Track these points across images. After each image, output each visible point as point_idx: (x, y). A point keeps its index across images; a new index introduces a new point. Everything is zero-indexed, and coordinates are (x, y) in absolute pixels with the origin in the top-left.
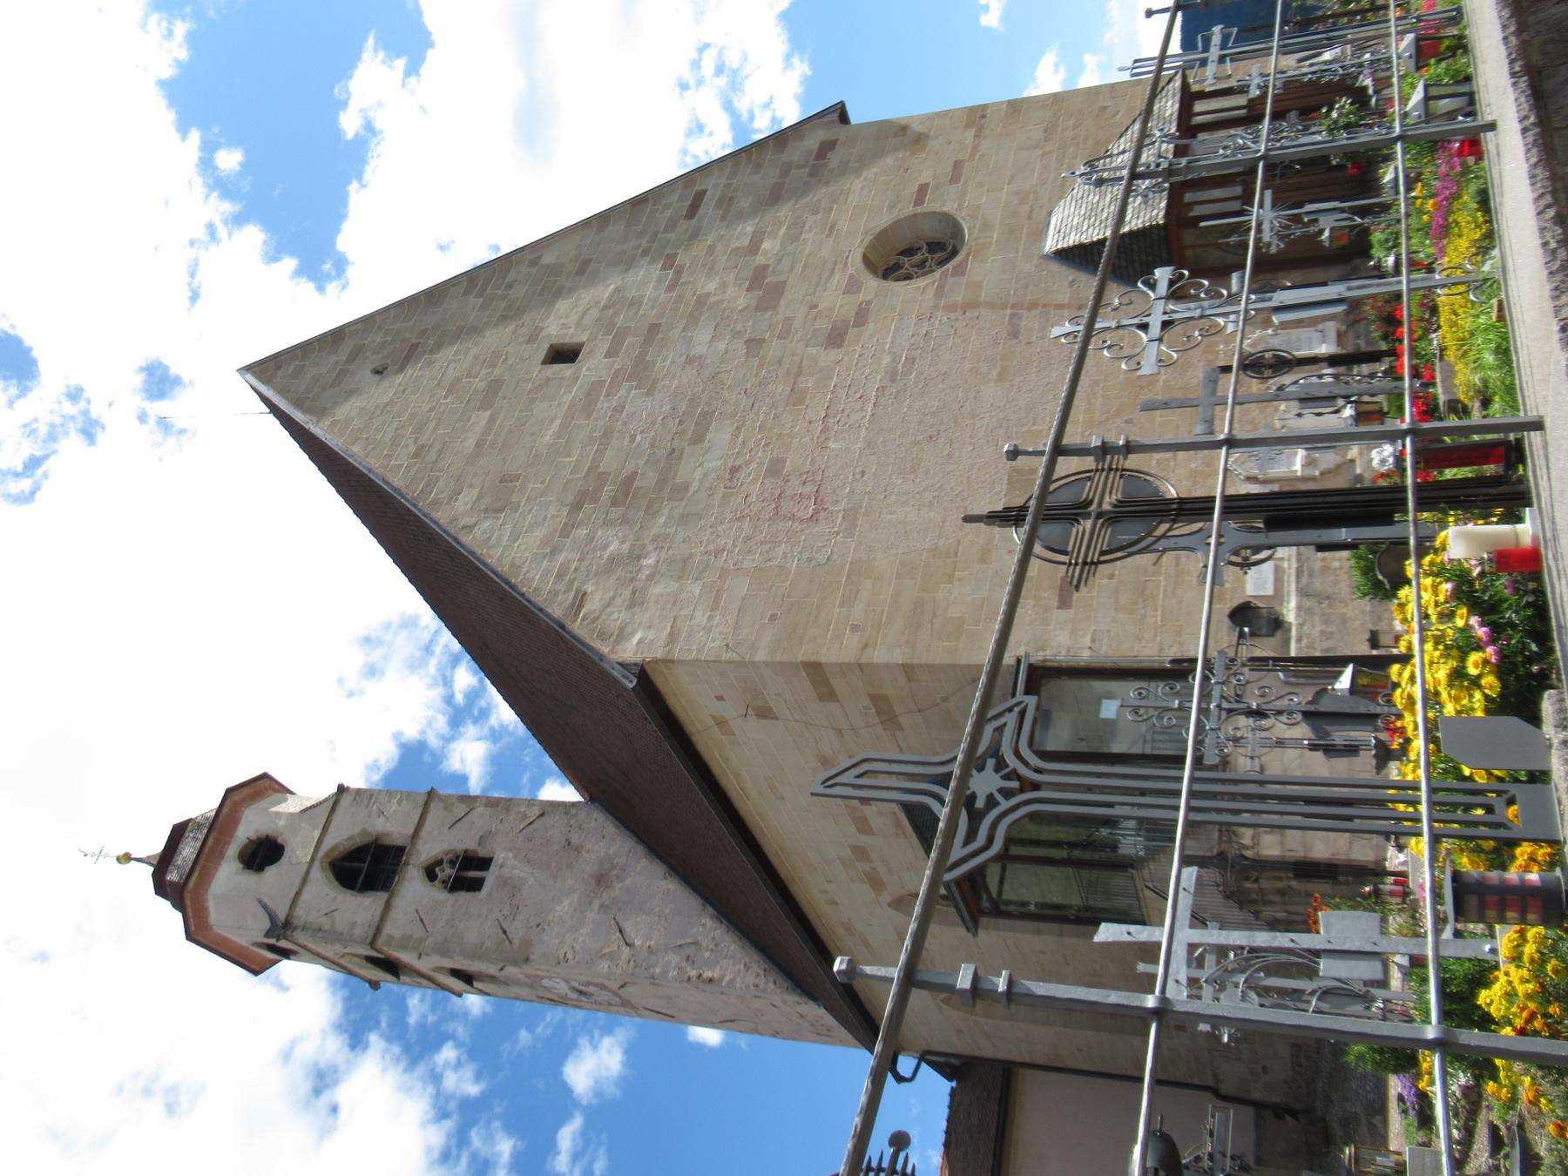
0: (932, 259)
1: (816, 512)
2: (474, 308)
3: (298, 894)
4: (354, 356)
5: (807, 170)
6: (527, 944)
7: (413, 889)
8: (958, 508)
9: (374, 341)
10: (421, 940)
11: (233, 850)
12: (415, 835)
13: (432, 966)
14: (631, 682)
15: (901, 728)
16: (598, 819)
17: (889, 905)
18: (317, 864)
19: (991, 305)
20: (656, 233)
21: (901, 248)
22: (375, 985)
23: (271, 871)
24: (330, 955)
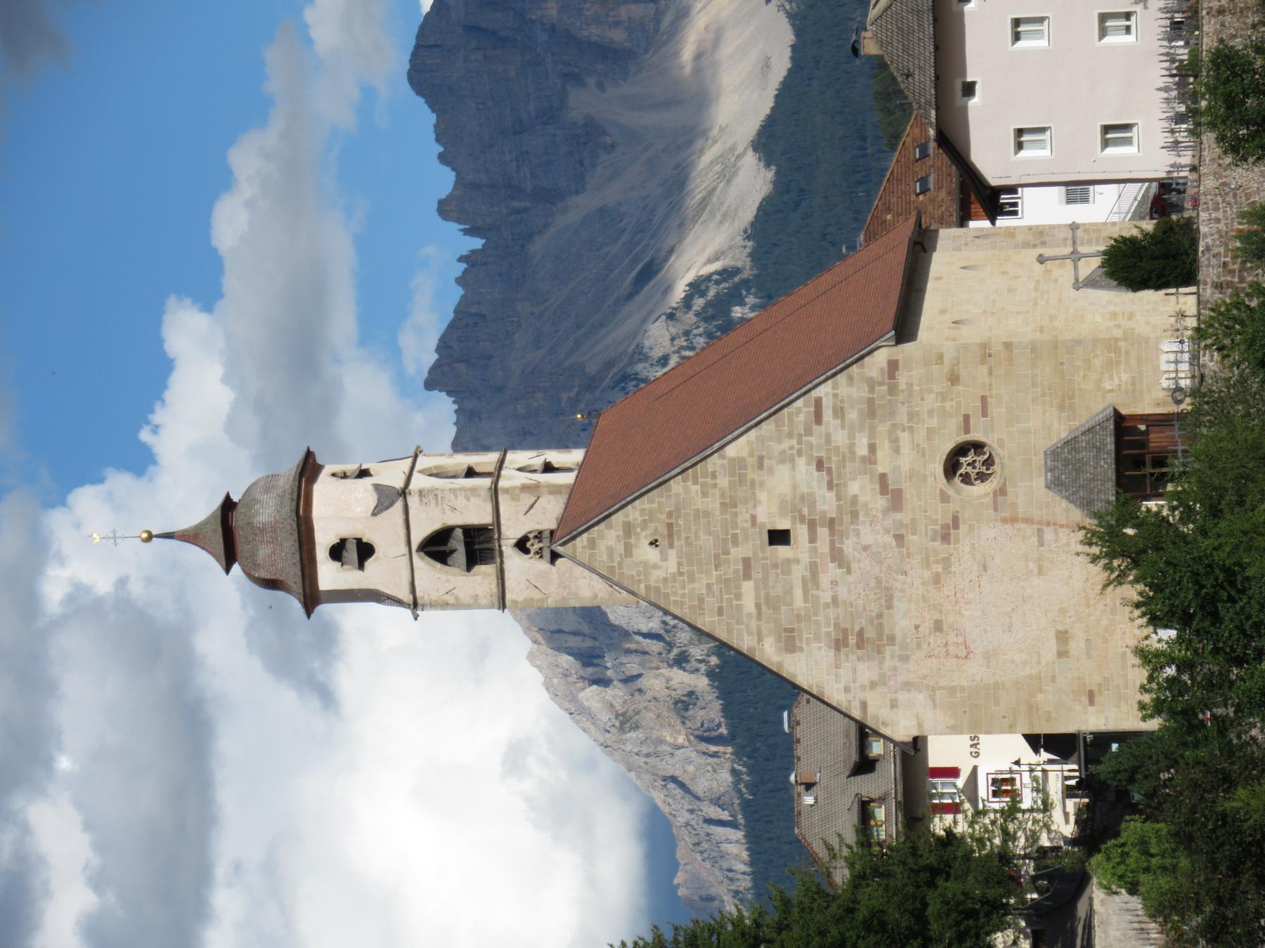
2: (697, 494)
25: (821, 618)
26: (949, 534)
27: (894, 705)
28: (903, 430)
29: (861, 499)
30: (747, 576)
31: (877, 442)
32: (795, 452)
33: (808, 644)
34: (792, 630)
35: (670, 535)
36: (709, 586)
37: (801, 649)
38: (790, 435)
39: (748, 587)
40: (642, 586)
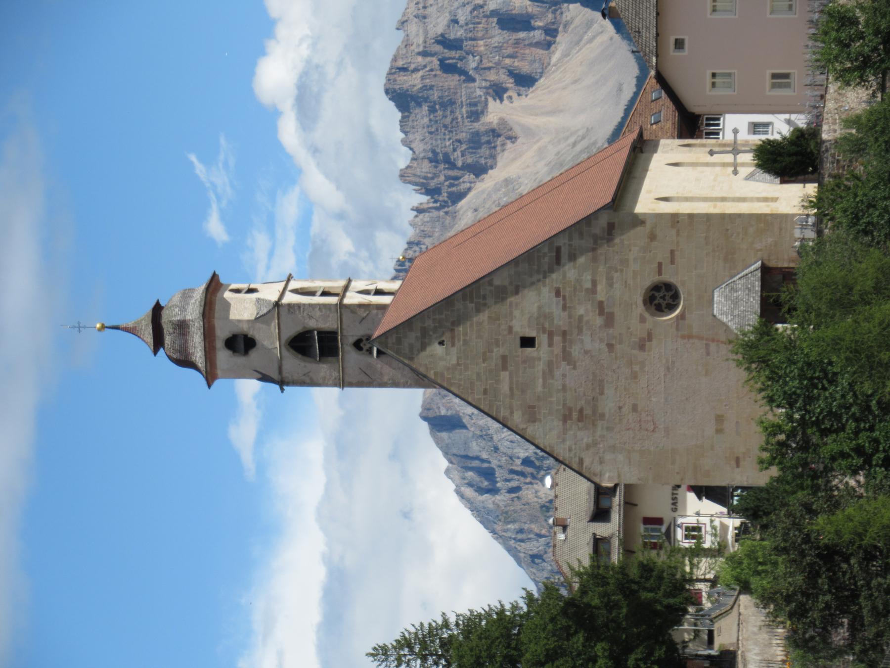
1: (655, 428)
2: (472, 308)
11: (220, 344)
18: (283, 348)
25: (554, 399)
26: (645, 345)
27: (601, 462)
28: (616, 271)
29: (585, 319)
30: (504, 368)
31: (598, 279)
34: (533, 407)
36: (478, 374)
37: (540, 421)
38: (538, 272)
40: (432, 372)
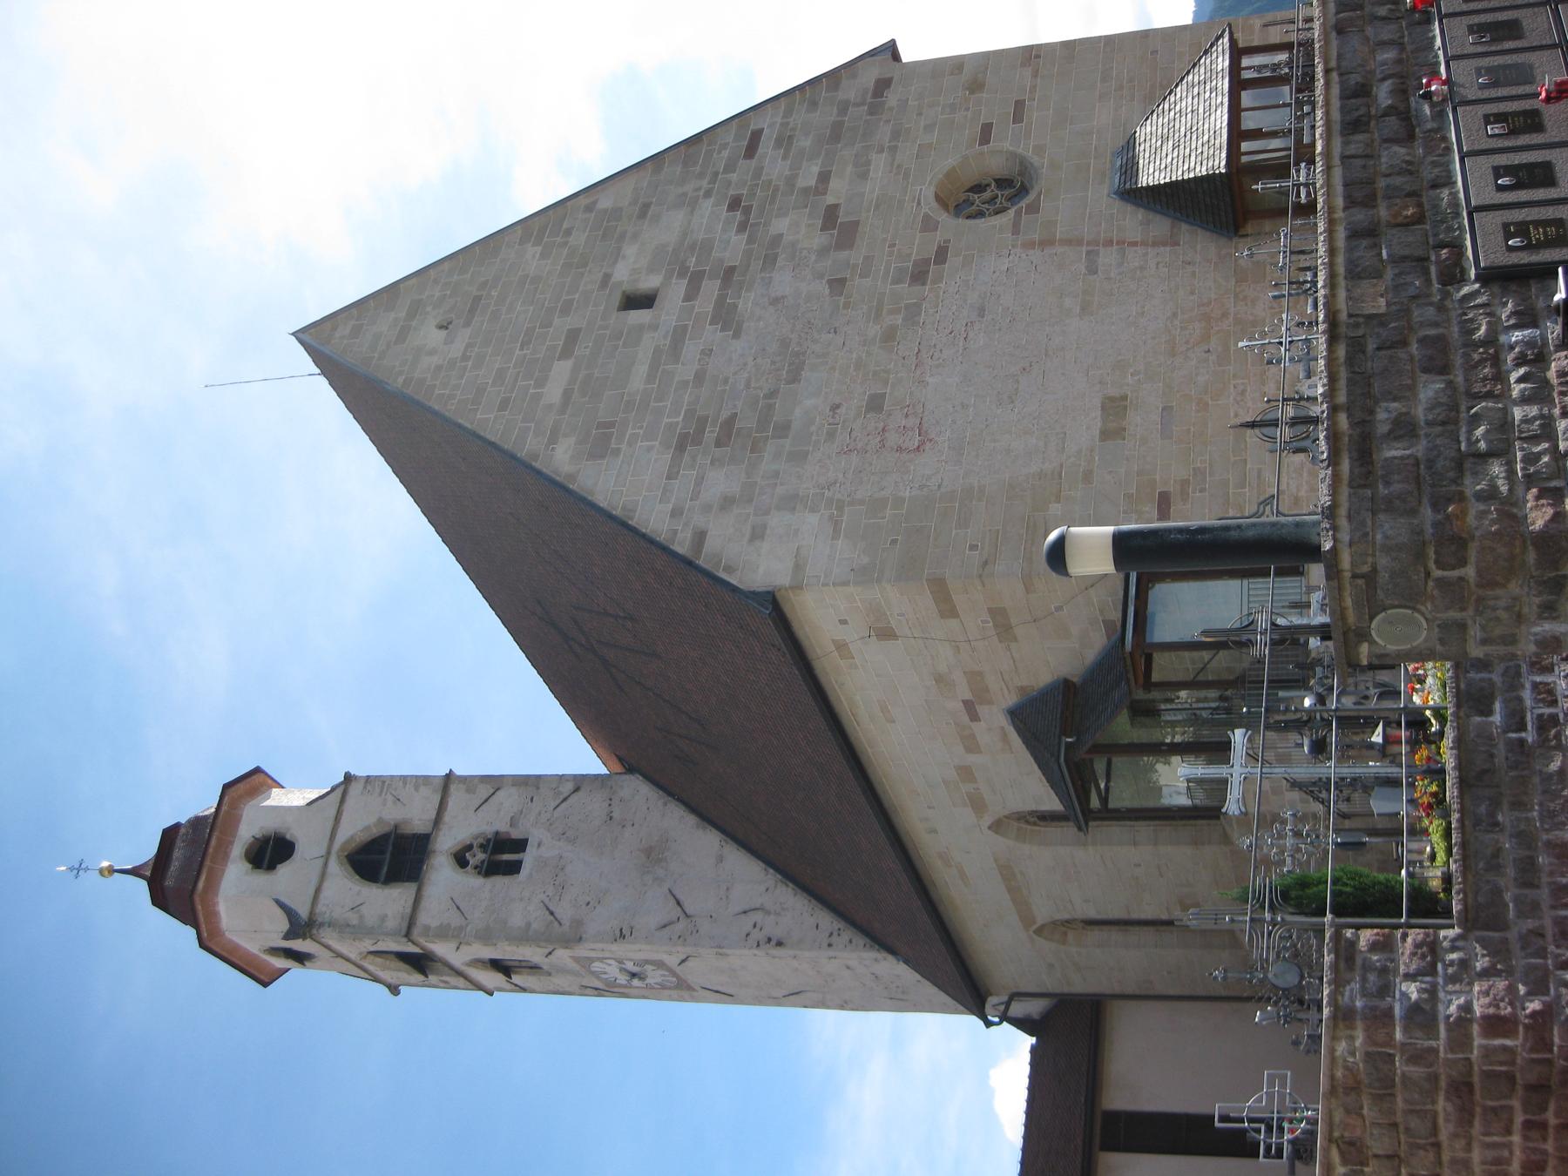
0: (1002, 195)
1: (922, 443)
2: (534, 256)
3: (318, 891)
4: (415, 311)
5: (866, 108)
6: (578, 923)
7: (442, 876)
8: (1057, 434)
9: (433, 296)
10: (461, 928)
11: (238, 850)
12: (438, 821)
13: (468, 958)
14: (767, 609)
15: (1015, 639)
16: (638, 791)
17: (990, 828)
19: (1068, 242)
20: (716, 174)
21: (966, 188)
22: (394, 990)
23: (284, 870)
24: (353, 956)
27: (758, 534)
28: (881, 151)
30: (566, 353)
32: (701, 193)
33: (630, 444)
34: (612, 425)
35: (472, 311)
38: (701, 175)
39: (561, 371)
